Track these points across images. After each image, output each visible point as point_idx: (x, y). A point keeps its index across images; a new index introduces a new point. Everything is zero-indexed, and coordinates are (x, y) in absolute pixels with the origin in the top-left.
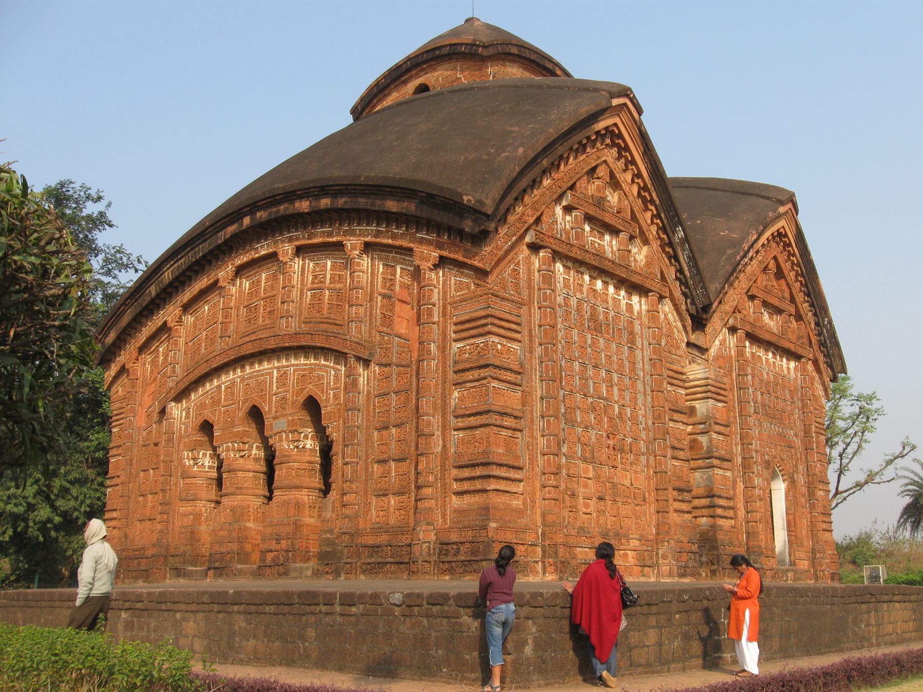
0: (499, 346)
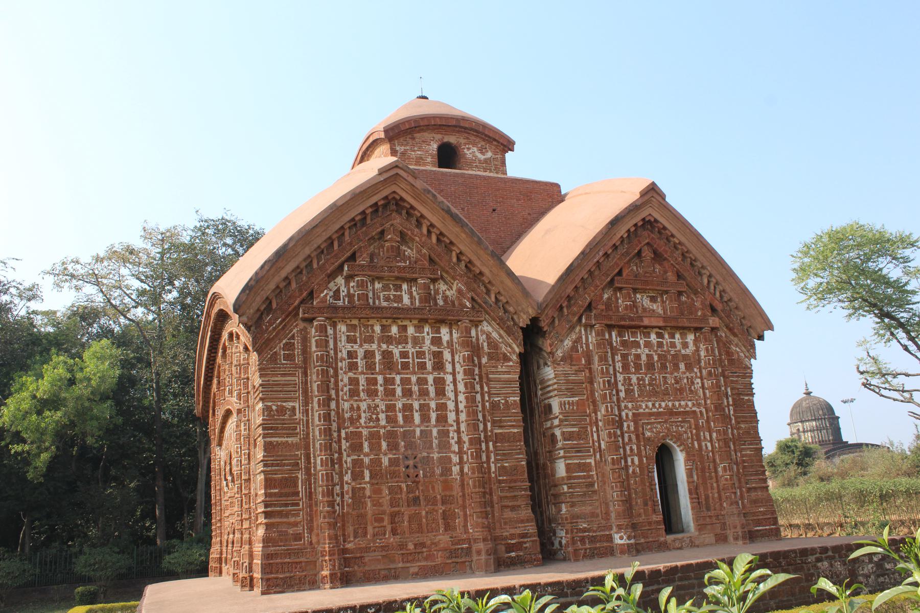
0: (274, 408)
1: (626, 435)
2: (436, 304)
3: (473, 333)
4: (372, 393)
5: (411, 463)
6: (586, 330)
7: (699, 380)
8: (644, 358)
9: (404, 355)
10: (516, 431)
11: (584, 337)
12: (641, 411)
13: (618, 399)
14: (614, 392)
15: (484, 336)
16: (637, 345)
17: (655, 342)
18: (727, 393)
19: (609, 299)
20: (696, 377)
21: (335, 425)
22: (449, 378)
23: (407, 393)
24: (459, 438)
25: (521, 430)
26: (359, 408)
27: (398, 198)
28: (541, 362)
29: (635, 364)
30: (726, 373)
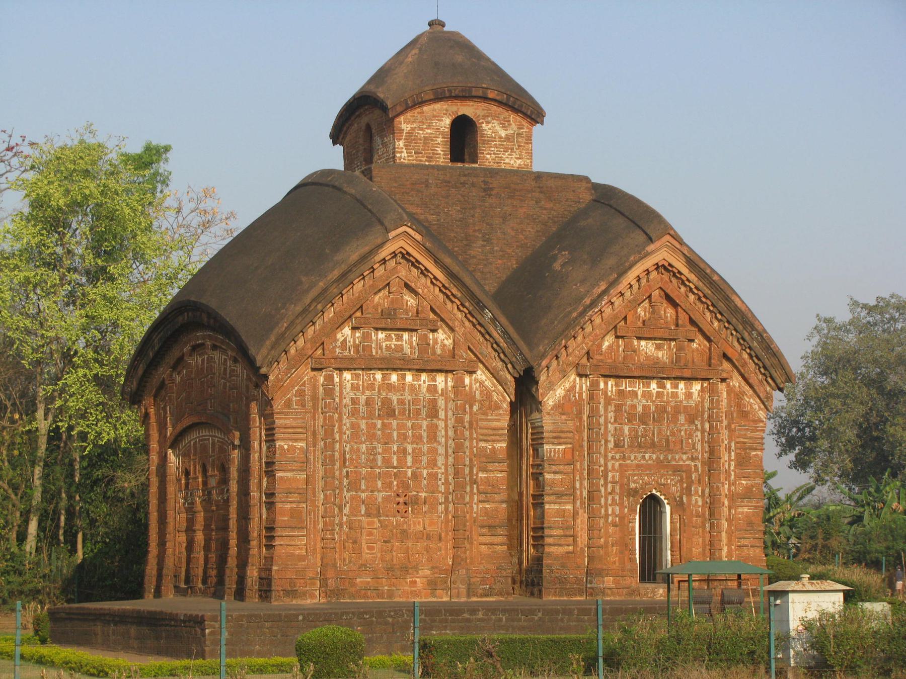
0: (286, 447)
1: (610, 485)
2: (434, 353)
3: (467, 380)
4: (372, 437)
5: (401, 500)
6: (581, 380)
7: (699, 434)
8: (640, 409)
9: (401, 402)
10: (499, 475)
11: (578, 386)
12: (628, 462)
13: (606, 448)
14: (603, 442)
15: (478, 385)
16: (635, 394)
17: (654, 392)
18: (730, 447)
19: (610, 347)
20: (697, 429)
21: (337, 465)
22: (442, 424)
23: (403, 437)
24: (446, 479)
25: (504, 474)
26: (358, 450)
27: (405, 252)
28: (534, 406)
29: (629, 414)
30: (733, 426)
